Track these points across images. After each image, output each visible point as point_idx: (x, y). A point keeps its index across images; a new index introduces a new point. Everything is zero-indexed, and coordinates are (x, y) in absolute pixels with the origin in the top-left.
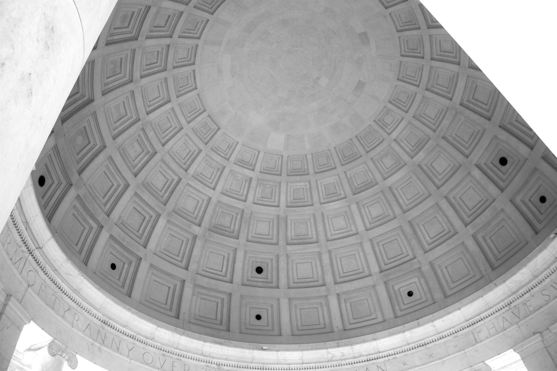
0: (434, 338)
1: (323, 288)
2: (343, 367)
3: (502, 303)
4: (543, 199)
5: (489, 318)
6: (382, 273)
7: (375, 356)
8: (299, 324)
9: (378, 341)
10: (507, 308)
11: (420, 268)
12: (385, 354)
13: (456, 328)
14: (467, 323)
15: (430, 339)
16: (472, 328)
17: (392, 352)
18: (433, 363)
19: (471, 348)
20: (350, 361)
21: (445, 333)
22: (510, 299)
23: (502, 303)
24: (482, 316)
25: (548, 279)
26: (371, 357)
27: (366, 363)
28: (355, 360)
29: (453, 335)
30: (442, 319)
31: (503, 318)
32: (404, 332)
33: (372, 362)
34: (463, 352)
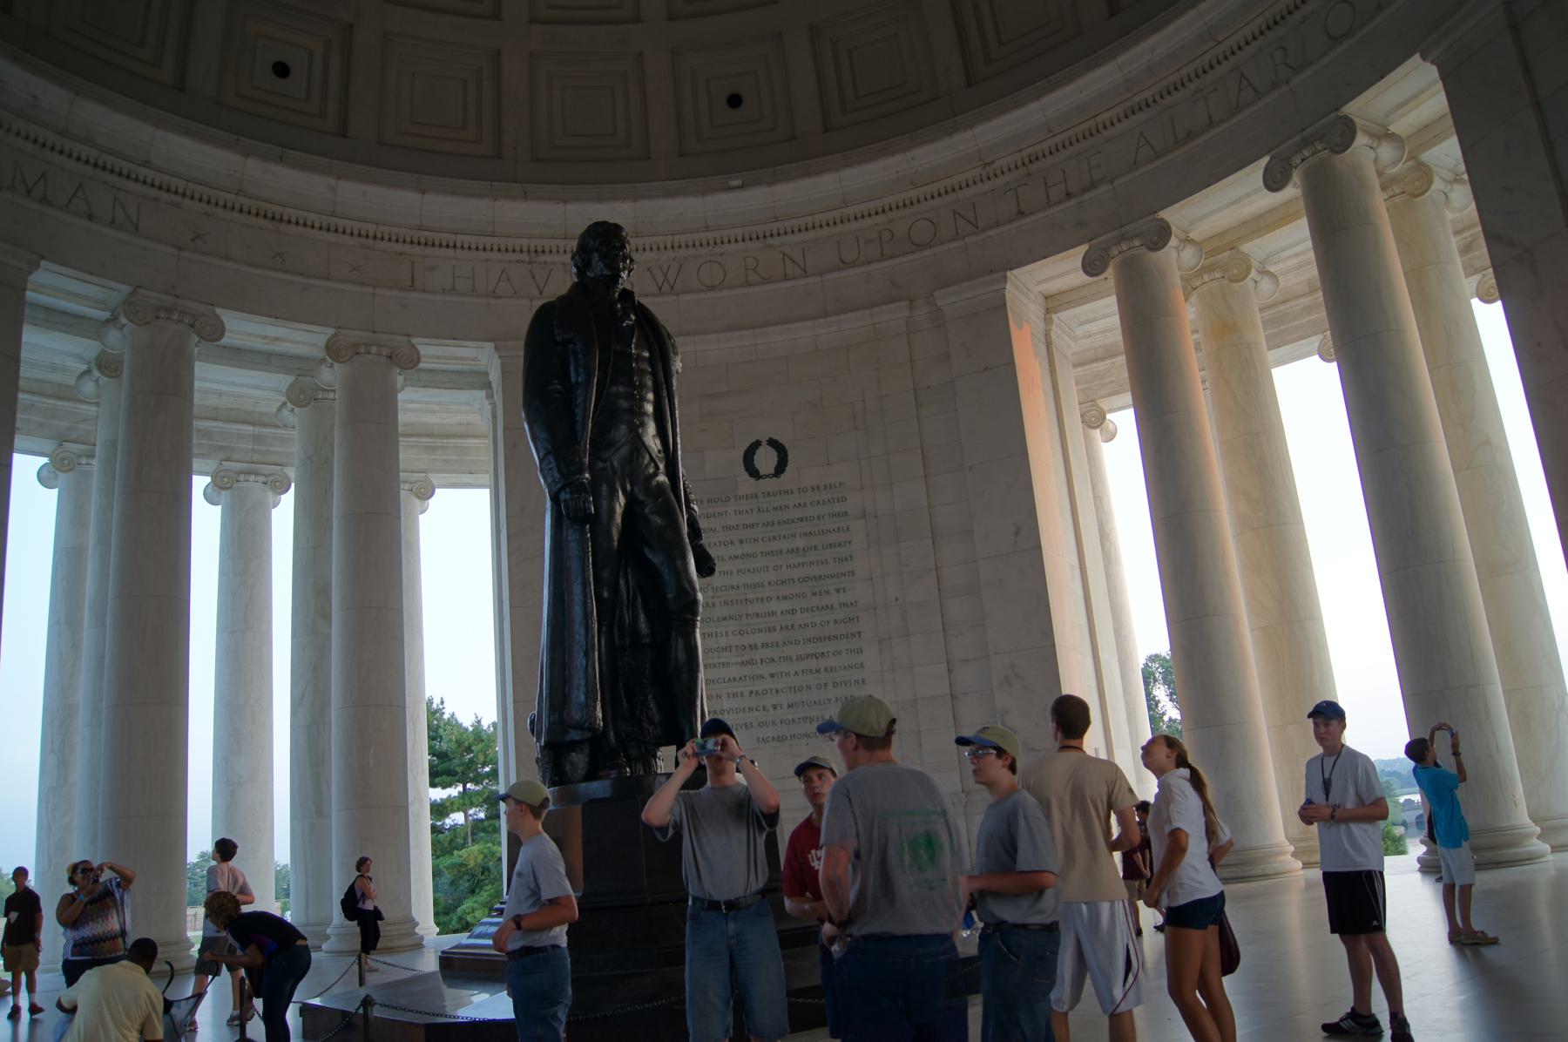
0: (311, 217)
3: (525, 242)
4: (735, 101)
10: (525, 257)
11: (351, 26)
12: (159, 178)
13: (382, 228)
15: (302, 214)
16: (417, 249)
17: (181, 185)
18: (280, 275)
21: (348, 224)
22: (547, 243)
23: (525, 242)
24: (460, 239)
25: (652, 255)
26: (110, 160)
27: (89, 170)
29: (363, 240)
32: (247, 156)
33: (107, 176)
34: (370, 290)
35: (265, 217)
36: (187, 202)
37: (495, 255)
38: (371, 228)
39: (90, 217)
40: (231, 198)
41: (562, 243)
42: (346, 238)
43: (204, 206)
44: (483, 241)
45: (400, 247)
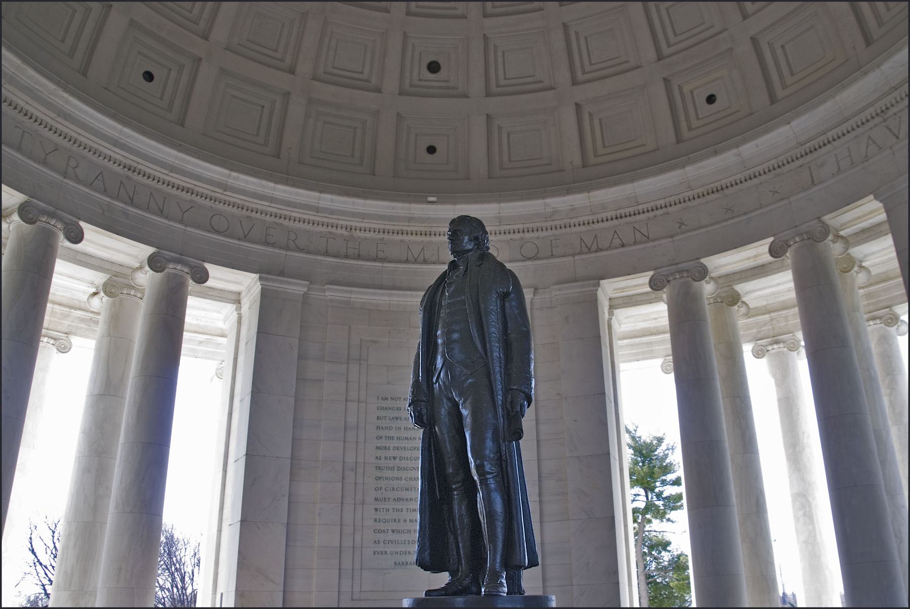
1: (550, 93)
2: (573, 229)
3: (871, 110)
5: (843, 140)
6: (661, 62)
7: (631, 210)
8: (506, 158)
9: (636, 184)
10: (878, 120)
12: (649, 206)
14: (802, 150)
15: (732, 179)
17: (662, 202)
19: (802, 195)
20: (586, 219)
21: (760, 168)
23: (871, 110)
24: (830, 135)
26: (622, 212)
27: (615, 222)
28: (595, 217)
29: (773, 172)
30: (754, 142)
31: (869, 137)
32: (684, 167)
33: (625, 220)
34: (785, 202)
35: (713, 192)
36: (670, 209)
37: (859, 131)
38: (774, 162)
39: (623, 246)
40: (690, 194)
41: (896, 94)
42: (764, 177)
43: (679, 206)
44: (844, 128)
45: (797, 163)
